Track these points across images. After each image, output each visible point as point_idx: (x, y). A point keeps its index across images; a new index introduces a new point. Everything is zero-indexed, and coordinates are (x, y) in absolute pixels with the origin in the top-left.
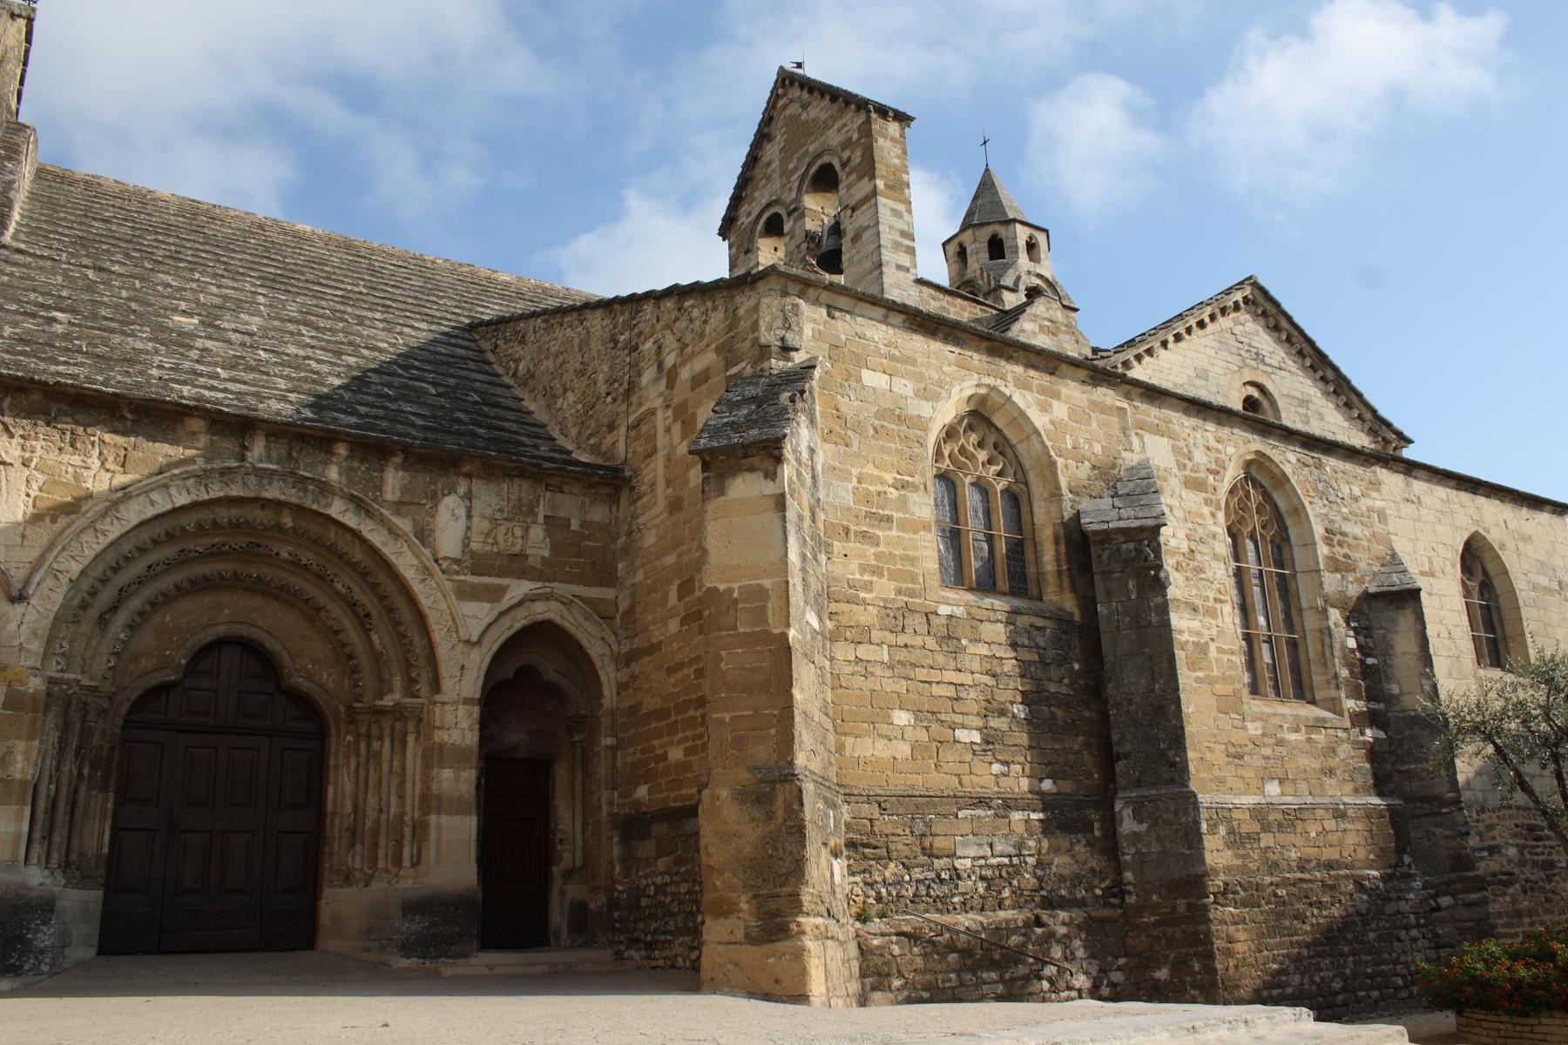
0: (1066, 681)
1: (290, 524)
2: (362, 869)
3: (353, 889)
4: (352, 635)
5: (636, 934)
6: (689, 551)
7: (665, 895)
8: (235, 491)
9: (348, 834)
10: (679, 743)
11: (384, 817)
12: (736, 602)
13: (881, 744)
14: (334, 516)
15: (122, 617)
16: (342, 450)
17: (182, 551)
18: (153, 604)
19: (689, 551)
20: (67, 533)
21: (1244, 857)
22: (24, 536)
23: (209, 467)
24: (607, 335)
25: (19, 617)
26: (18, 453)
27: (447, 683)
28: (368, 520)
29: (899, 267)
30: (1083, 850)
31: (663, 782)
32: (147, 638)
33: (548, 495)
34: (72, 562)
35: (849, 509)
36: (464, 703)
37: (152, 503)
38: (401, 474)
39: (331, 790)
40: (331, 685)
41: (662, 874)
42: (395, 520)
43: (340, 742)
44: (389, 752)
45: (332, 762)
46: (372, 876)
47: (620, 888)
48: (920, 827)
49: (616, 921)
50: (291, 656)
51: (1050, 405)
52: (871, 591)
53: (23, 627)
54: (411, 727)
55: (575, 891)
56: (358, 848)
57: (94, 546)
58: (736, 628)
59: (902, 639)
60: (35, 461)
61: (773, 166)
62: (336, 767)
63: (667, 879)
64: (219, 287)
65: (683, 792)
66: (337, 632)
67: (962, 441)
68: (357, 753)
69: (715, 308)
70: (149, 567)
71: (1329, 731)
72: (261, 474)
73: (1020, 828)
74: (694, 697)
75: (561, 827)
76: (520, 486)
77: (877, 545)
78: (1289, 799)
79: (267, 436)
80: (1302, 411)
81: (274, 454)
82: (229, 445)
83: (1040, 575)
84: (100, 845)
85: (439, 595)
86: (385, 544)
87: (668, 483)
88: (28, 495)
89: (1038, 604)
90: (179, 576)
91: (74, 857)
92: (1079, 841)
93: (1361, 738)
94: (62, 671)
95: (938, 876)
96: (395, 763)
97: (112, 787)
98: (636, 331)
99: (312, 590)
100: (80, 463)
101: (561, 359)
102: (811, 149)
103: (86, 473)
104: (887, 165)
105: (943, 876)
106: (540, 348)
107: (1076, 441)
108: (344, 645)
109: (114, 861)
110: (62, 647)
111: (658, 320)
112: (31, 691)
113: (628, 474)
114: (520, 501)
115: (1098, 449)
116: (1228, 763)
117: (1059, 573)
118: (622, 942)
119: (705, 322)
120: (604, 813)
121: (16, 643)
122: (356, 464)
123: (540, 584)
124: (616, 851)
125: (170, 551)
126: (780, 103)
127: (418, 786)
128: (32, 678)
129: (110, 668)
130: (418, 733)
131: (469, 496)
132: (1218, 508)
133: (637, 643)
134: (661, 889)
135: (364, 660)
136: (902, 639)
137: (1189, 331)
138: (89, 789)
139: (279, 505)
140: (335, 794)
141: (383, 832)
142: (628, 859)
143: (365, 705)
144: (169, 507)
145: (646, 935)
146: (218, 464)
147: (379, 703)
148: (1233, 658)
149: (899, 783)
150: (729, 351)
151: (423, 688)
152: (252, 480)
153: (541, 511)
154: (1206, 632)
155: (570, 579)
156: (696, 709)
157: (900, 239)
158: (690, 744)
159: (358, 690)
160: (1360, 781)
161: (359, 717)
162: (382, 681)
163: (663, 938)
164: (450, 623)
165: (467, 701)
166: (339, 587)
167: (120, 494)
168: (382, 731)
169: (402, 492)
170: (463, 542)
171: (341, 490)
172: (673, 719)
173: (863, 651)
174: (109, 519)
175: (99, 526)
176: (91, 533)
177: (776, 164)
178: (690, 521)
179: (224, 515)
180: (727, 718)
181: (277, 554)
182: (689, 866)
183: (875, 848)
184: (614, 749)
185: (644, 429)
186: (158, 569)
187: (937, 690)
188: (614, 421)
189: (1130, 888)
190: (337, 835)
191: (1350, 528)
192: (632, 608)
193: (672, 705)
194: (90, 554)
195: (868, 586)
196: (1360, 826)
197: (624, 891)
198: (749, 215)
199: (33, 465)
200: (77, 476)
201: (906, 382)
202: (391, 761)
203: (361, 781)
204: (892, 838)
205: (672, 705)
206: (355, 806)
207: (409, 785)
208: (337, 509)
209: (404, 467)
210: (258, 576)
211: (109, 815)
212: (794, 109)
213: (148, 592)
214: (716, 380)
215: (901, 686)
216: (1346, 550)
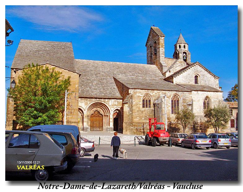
29: (162, 56)
43: (104, 117)
109: (91, 125)
149: (137, 122)
155: (119, 106)
208: (103, 102)
212: (152, 32)
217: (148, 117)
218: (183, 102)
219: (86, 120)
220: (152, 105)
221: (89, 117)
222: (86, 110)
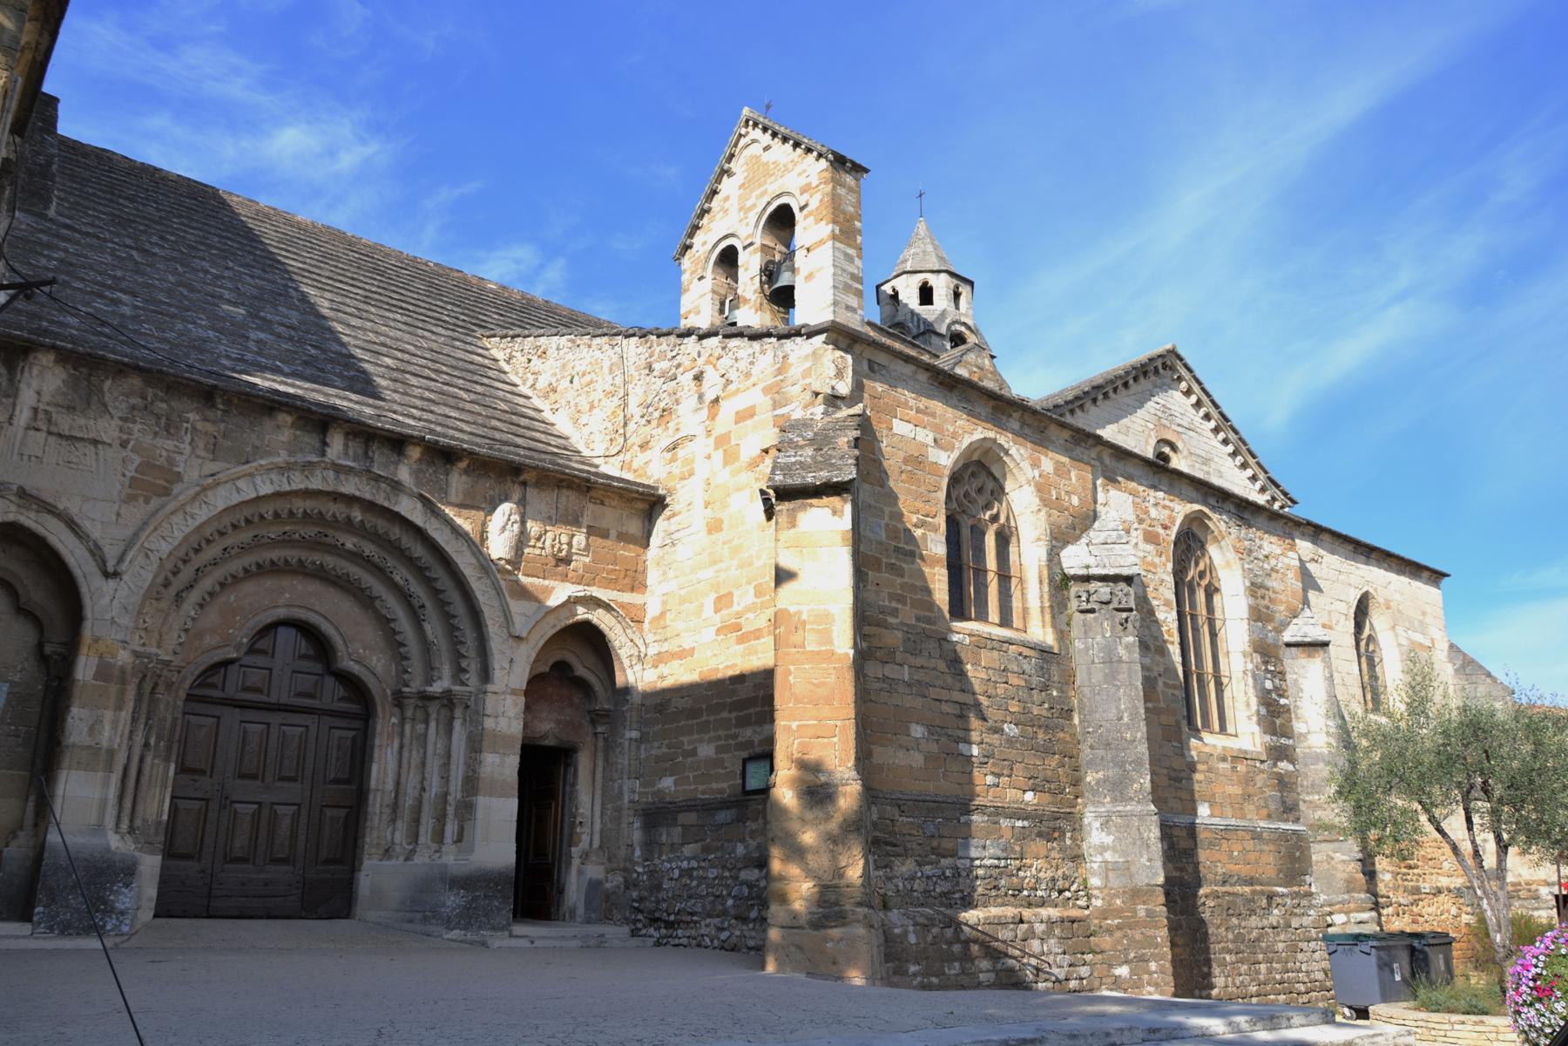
0: (1046, 706)
1: (359, 518)
2: (401, 844)
3: (393, 862)
4: (404, 624)
5: (657, 915)
6: (727, 569)
7: (691, 877)
8: (316, 483)
9: (388, 810)
10: (710, 741)
11: (426, 796)
12: (804, 623)
13: (900, 754)
14: (403, 513)
15: (194, 597)
16: (415, 453)
17: (255, 537)
18: (222, 585)
19: (727, 569)
20: (160, 513)
21: (1182, 870)
22: (118, 515)
23: (292, 460)
24: (643, 363)
25: (112, 591)
26: (117, 434)
27: (498, 674)
28: (433, 519)
30: (1057, 856)
31: (691, 775)
32: (212, 617)
33: (591, 506)
34: (162, 542)
35: (880, 543)
36: (511, 694)
37: (238, 490)
38: (464, 478)
39: (375, 768)
40: (379, 669)
41: (689, 859)
42: (459, 521)
43: (385, 721)
44: (434, 735)
45: (377, 742)
46: (413, 851)
47: (640, 870)
48: (931, 829)
49: (634, 900)
50: (345, 641)
51: (1040, 460)
52: (897, 617)
53: (115, 602)
54: (458, 713)
55: (594, 871)
56: (399, 824)
57: (183, 528)
58: (803, 646)
59: (919, 661)
60: (132, 443)
61: (730, 202)
62: (380, 746)
63: (694, 864)
64: (252, 277)
65: (714, 786)
66: (389, 621)
67: (967, 487)
68: (402, 735)
69: (763, 352)
70: (225, 550)
71: (1249, 762)
72: (338, 469)
73: (1008, 835)
74: (729, 700)
75: (581, 811)
76: (568, 497)
77: (902, 576)
78: (1216, 820)
79: (347, 435)
80: (1205, 468)
81: (351, 452)
82: (311, 440)
83: (1025, 611)
84: (160, 813)
85: (493, 592)
86: (447, 543)
87: (707, 505)
88: (124, 475)
89: (1024, 635)
90: (249, 560)
91: (138, 823)
92: (1053, 848)
93: (1275, 770)
94: (144, 645)
95: (944, 874)
96: (438, 746)
97: (174, 757)
98: (675, 362)
99: (369, 580)
100: (172, 448)
101: (587, 378)
102: (770, 190)
103: (178, 457)
104: (844, 213)
105: (947, 874)
106: (564, 366)
107: (1059, 494)
108: (395, 632)
109: (172, 828)
110: (145, 622)
111: (699, 355)
112: (120, 663)
113: (661, 492)
114: (567, 510)
115: (1075, 501)
116: (1170, 786)
117: (1042, 608)
118: (639, 921)
119: (752, 363)
120: (626, 800)
121: (108, 617)
122: (424, 467)
123: (581, 587)
124: (638, 836)
125: (245, 536)
126: (743, 142)
127: (462, 768)
128: (121, 651)
129: (180, 644)
130: (465, 719)
131: (522, 503)
132: (1168, 561)
133: (665, 647)
134: (688, 873)
135: (413, 648)
136: (919, 661)
137: (1115, 390)
138: (155, 757)
139: (351, 500)
140: (379, 773)
141: (426, 808)
142: (650, 846)
143: (414, 690)
144: (254, 495)
145: (669, 915)
146: (300, 458)
147: (429, 689)
148: (1177, 693)
150: (778, 393)
151: (472, 679)
152: (331, 474)
153: (586, 520)
154: (1155, 668)
156: (730, 712)
157: (850, 282)
158: (722, 742)
159: (406, 676)
160: (1273, 807)
161: (407, 701)
162: (432, 669)
163: (688, 918)
164: (502, 619)
165: (514, 692)
166: (397, 578)
167: (210, 480)
168: (427, 715)
169: (465, 496)
171: (411, 490)
172: (705, 718)
173: (890, 671)
174: (197, 504)
175: (188, 509)
176: (180, 515)
177: (734, 200)
178: (729, 542)
179: (300, 505)
180: (794, 725)
181: (343, 545)
182: (719, 854)
183: (895, 846)
184: (640, 741)
185: (680, 452)
186: (233, 552)
187: (946, 708)
188: (648, 443)
189: (1095, 892)
190: (378, 811)
191: (1269, 583)
192: (663, 614)
193: (704, 707)
194: (179, 535)
195: (894, 612)
196: (1272, 847)
197: (643, 874)
198: (704, 243)
199: (130, 447)
200: (170, 461)
201: (928, 433)
202: (435, 743)
203: (405, 762)
204: (908, 838)
205: (704, 707)
206: (398, 784)
207: (453, 767)
209: (466, 472)
210: (321, 564)
211: (170, 783)
212: (756, 149)
213: (219, 573)
214: (763, 417)
215: (918, 703)
216: (1266, 602)
217: (1010, 729)
218: (1259, 615)
219: (106, 736)
220: (1032, 593)
221: (170, 705)
222: (140, 574)
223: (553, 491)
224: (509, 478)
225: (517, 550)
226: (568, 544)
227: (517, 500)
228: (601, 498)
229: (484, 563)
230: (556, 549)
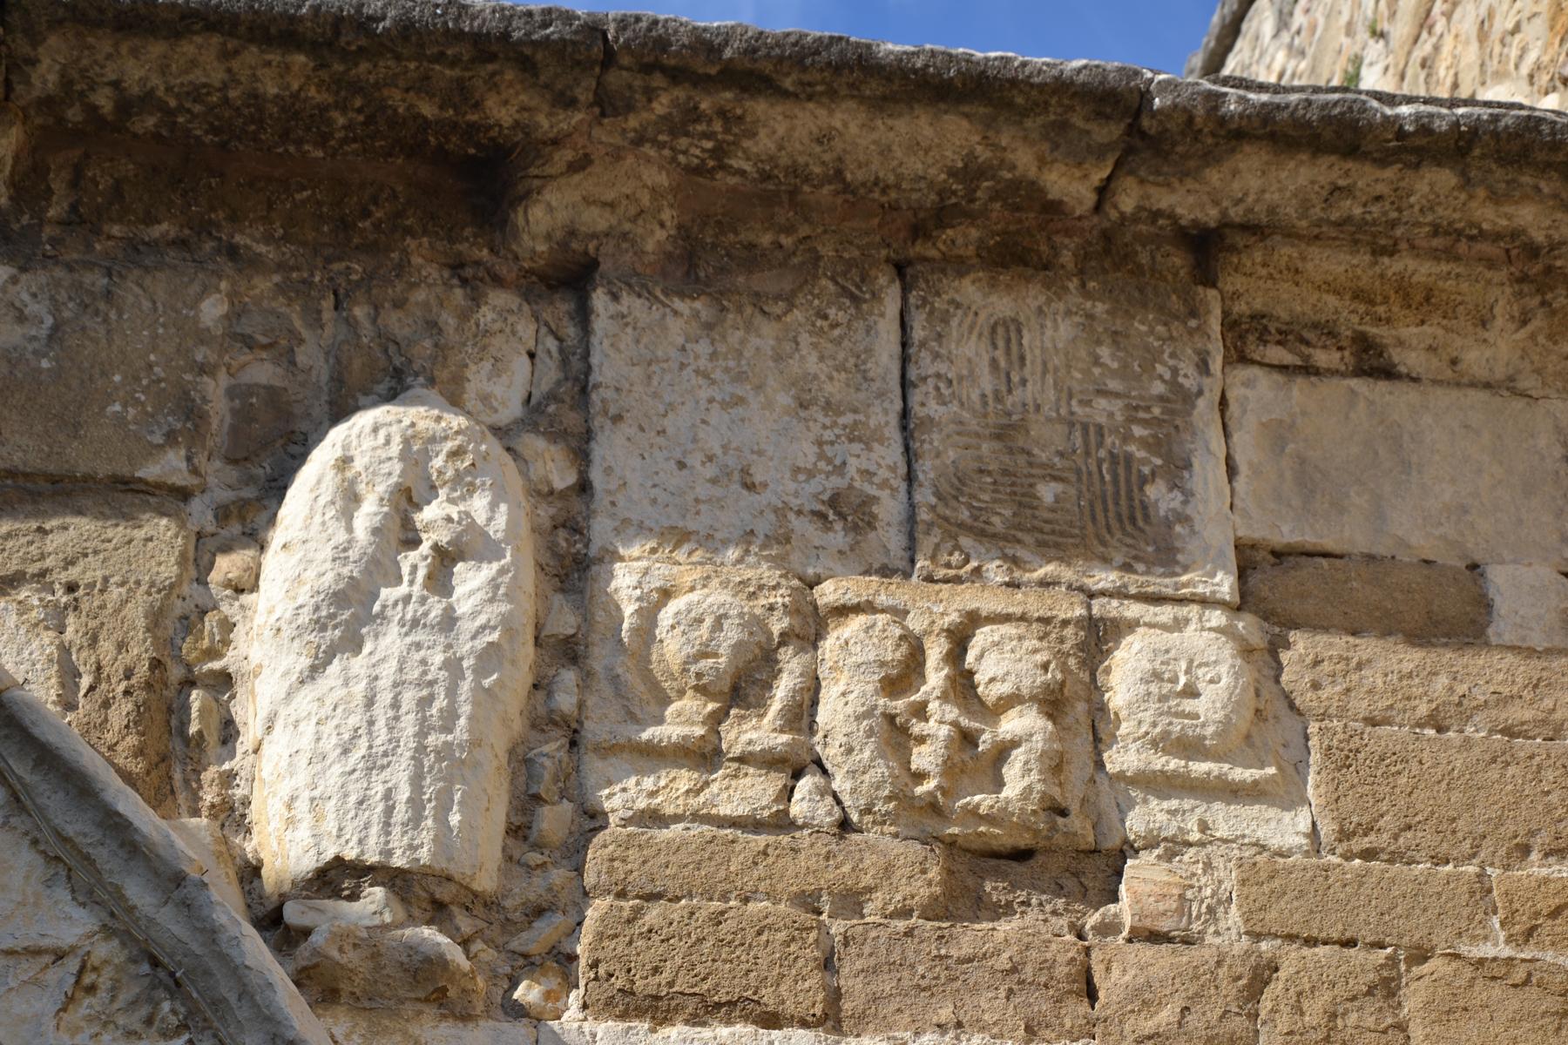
76: (1006, 332)
170: (522, 762)
223: (857, 298)
224: (421, 254)
225: (527, 802)
226: (1052, 703)
227: (511, 409)
228: (1350, 319)
229: (169, 924)
230: (924, 758)
